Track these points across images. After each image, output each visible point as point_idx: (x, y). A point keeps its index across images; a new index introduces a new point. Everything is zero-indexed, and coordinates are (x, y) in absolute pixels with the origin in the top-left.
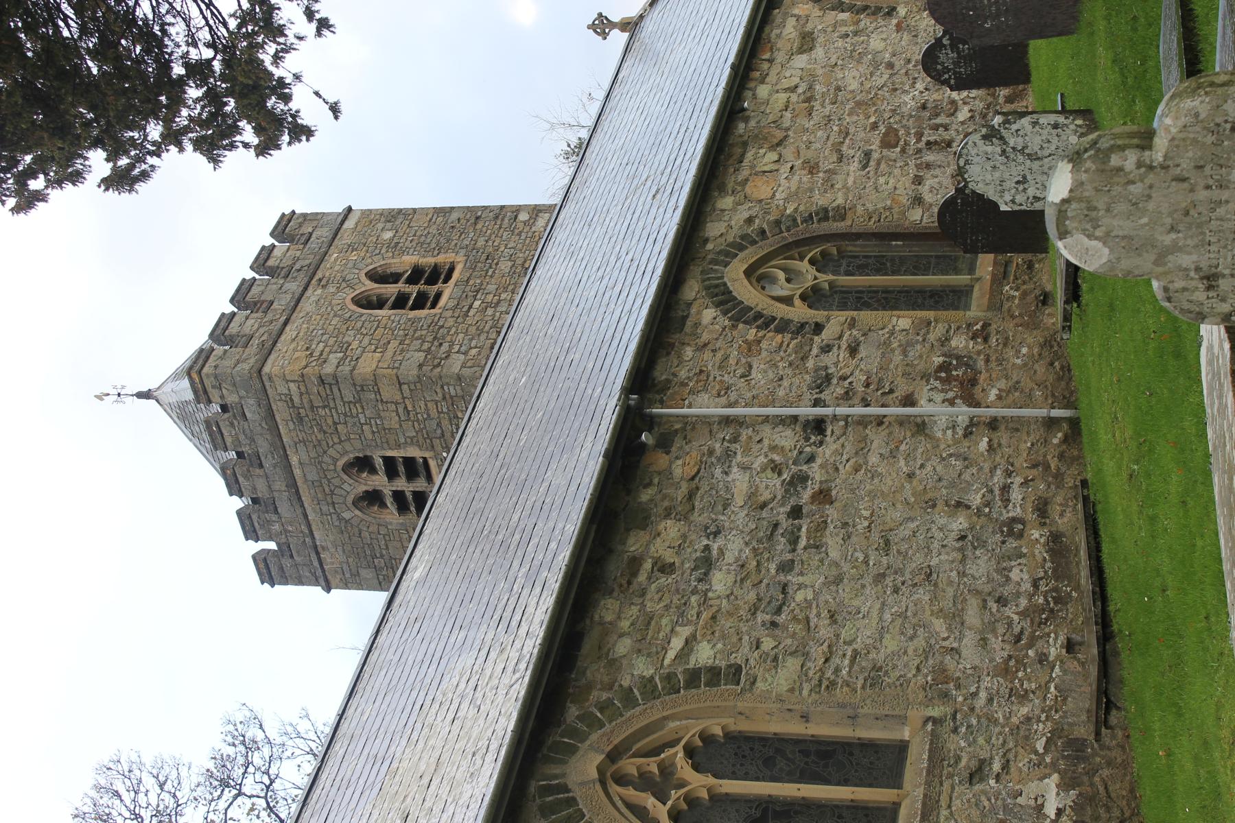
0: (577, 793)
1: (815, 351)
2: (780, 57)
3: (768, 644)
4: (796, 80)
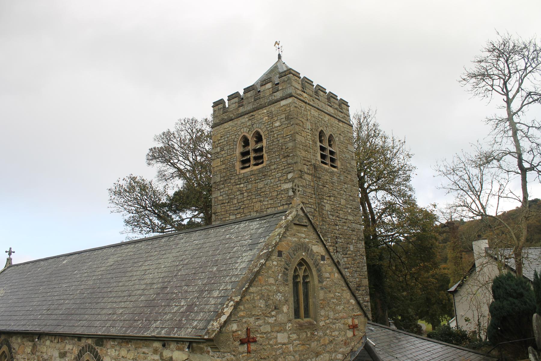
2: (58, 346)
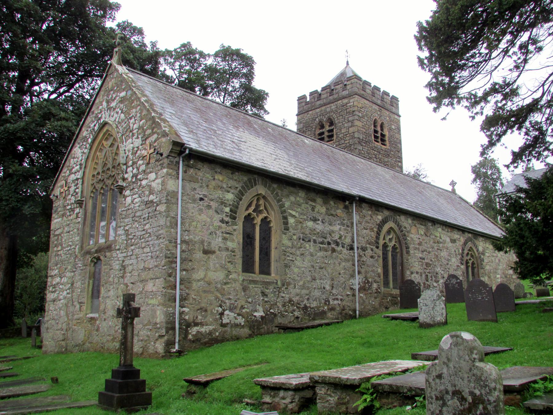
0: (254, 188)
1: (372, 247)
2: (449, 234)
3: (295, 237)
4: (443, 238)
